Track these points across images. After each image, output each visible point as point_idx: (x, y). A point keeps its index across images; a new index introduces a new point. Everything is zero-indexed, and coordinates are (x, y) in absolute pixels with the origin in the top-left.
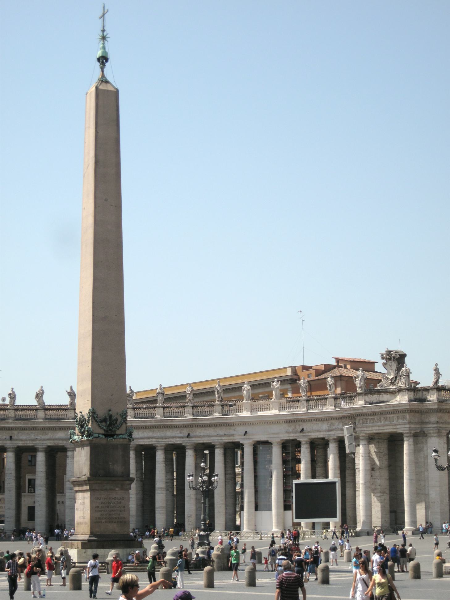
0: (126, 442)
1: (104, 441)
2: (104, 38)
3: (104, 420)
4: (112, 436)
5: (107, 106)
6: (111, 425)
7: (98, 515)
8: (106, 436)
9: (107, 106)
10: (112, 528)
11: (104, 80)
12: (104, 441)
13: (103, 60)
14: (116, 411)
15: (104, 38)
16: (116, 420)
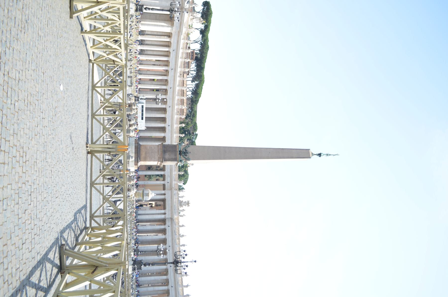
0: (178, 159)
1: (178, 150)
2: (327, 155)
3: (186, 151)
4: (180, 154)
5: (304, 154)
6: (184, 150)
7: (148, 148)
8: (180, 151)
9: (304, 154)
10: (143, 154)
11: (313, 154)
12: (178, 150)
13: (320, 155)
14: (189, 155)
15: (327, 155)
16: (186, 156)
